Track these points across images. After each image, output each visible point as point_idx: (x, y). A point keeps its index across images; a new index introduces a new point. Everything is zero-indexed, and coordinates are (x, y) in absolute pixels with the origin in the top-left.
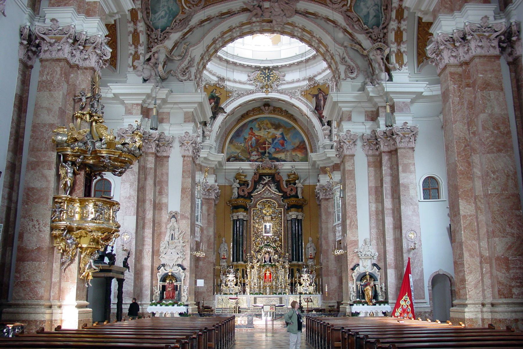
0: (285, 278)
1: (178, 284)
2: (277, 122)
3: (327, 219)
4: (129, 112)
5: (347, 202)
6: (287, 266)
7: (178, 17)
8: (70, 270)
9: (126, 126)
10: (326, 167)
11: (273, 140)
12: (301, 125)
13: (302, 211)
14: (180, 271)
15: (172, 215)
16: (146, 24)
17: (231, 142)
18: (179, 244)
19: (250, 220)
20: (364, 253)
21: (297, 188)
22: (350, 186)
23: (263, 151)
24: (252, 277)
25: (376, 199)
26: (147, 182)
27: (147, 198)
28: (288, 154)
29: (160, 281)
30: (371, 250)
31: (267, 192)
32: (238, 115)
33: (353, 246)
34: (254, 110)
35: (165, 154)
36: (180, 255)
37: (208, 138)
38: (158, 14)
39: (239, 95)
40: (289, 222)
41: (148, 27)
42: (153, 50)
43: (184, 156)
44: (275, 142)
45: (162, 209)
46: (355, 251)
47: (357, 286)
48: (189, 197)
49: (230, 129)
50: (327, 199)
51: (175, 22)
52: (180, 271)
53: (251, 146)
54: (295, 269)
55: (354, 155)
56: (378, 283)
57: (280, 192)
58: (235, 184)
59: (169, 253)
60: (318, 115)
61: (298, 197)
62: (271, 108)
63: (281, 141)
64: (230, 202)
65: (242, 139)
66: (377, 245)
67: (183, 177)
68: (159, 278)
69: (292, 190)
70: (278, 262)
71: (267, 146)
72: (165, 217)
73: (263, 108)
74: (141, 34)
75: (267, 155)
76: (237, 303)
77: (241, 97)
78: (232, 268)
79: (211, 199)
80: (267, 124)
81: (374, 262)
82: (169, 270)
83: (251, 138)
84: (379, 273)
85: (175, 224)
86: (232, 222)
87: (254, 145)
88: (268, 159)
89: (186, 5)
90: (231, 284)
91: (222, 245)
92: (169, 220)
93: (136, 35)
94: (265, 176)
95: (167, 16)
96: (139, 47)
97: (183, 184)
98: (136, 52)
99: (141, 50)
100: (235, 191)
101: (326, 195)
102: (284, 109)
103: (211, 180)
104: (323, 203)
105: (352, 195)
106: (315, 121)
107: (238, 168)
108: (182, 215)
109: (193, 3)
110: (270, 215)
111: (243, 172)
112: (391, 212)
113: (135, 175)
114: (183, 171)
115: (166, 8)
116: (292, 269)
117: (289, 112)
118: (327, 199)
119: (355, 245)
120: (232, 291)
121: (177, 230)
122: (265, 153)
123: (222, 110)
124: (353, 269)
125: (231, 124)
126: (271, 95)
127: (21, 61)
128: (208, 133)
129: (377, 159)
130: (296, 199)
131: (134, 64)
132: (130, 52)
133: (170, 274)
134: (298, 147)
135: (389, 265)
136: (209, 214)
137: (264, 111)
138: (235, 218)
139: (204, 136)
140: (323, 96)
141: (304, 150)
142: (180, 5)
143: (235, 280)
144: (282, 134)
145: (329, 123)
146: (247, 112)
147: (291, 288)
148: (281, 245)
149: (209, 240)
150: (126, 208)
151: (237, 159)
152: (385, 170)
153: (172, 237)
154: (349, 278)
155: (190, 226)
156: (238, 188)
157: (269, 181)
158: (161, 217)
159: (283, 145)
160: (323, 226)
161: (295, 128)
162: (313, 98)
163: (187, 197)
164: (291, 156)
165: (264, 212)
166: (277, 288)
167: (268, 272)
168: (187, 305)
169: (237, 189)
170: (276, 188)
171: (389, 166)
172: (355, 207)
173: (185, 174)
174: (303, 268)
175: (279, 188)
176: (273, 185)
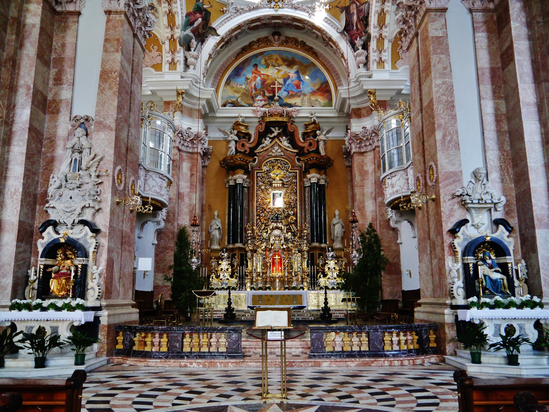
0: (301, 265)
1: (79, 261)
2: (290, 57)
3: (362, 180)
5: (434, 97)
6: (305, 248)
10: (359, 109)
11: (285, 81)
12: (323, 61)
13: (325, 173)
14: (86, 234)
15: (78, 123)
17: (228, 83)
18: (86, 179)
19: (253, 186)
20: (478, 196)
21: (318, 141)
22: (440, 66)
23: (271, 95)
24: (254, 265)
25: (494, 92)
26: (25, 52)
27: (21, 82)
28: (306, 98)
29: (41, 257)
30: (491, 191)
31: (276, 148)
32: (237, 46)
33: (451, 184)
34: (259, 40)
35: (71, 8)
36: (89, 202)
37: (192, 67)
39: (238, 11)
40: (307, 189)
43: (108, 13)
44: (287, 83)
45: (58, 112)
46: (458, 194)
47: (466, 266)
48: (116, 89)
49: (226, 66)
50: (362, 153)
52: (86, 234)
53: (256, 89)
54: (317, 253)
55: (444, 10)
56: (510, 259)
57: (294, 148)
58: (232, 135)
59: (65, 198)
60: (348, 38)
61: (319, 153)
62: (283, 38)
63: (296, 82)
64: (225, 160)
65: (242, 79)
66: (502, 181)
67: (106, 51)
68: (40, 250)
69: (310, 144)
70: (292, 242)
71: (276, 86)
72: (63, 125)
73: (271, 38)
75: (276, 98)
76: (229, 303)
77: (241, 14)
78: (226, 252)
79: (197, 153)
80: (277, 60)
81: (498, 215)
82: (64, 233)
83: (255, 78)
84: (511, 239)
85: (83, 140)
86: (227, 190)
87: (259, 87)
88: (277, 104)
90: (225, 275)
91: (213, 222)
92: (71, 134)
94: (274, 127)
97: (104, 62)
100: (232, 145)
101: (360, 148)
102: (300, 40)
103: (195, 126)
104: (357, 159)
105: (444, 83)
106: (344, 45)
107: (236, 115)
108: (100, 123)
110: (281, 180)
111: (243, 122)
112: (533, 110)
114: (106, 40)
116: (312, 255)
117: (308, 44)
118: (362, 153)
119: (454, 181)
120: (227, 284)
121: (86, 152)
122: (275, 96)
123: (214, 31)
124: (453, 232)
125: (228, 60)
126: (281, 12)
128: (193, 60)
129: (492, 17)
130: (317, 156)
133: (62, 240)
134: (318, 89)
135: (540, 220)
136: (192, 175)
137: (274, 42)
138: (232, 183)
139: (187, 66)
140: (357, 8)
141: (328, 94)
143: (230, 270)
144: (297, 72)
145: (365, 47)
146: (250, 43)
147: (311, 280)
148: (296, 220)
149: (191, 211)
151: (235, 104)
152: (516, 28)
153: (77, 165)
154: (446, 249)
155: (113, 145)
156: (236, 142)
157: (279, 134)
158: (56, 127)
159: (298, 87)
160: (357, 191)
161: (314, 65)
162: (342, 12)
163: (111, 88)
164: (309, 100)
165: (272, 175)
166: (290, 282)
167: (277, 257)
168: (99, 309)
169: (234, 142)
170: (289, 143)
171: (524, 20)
172: (451, 106)
173: (108, 45)
174: (329, 251)
175: (293, 142)
176: (284, 138)
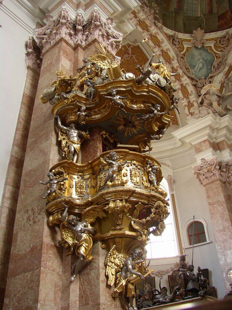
4: (198, 150)
7: (214, 63)
8: (89, 283)
9: (199, 163)
16: (189, 77)
38: (197, 66)
41: (192, 79)
42: (203, 92)
51: (214, 67)
74: (187, 87)
89: (217, 50)
93: (184, 89)
95: (205, 66)
96: (190, 97)
98: (189, 102)
99: (193, 98)
109: (223, 46)
113: (222, 205)
115: (201, 60)
127: (28, 68)
131: (191, 111)
132: (184, 105)
142: (213, 53)
150: (223, 241)
